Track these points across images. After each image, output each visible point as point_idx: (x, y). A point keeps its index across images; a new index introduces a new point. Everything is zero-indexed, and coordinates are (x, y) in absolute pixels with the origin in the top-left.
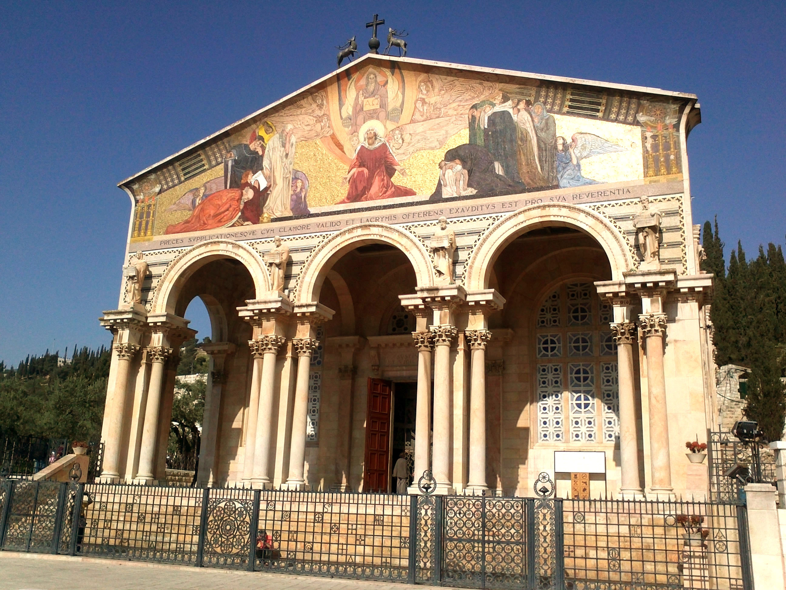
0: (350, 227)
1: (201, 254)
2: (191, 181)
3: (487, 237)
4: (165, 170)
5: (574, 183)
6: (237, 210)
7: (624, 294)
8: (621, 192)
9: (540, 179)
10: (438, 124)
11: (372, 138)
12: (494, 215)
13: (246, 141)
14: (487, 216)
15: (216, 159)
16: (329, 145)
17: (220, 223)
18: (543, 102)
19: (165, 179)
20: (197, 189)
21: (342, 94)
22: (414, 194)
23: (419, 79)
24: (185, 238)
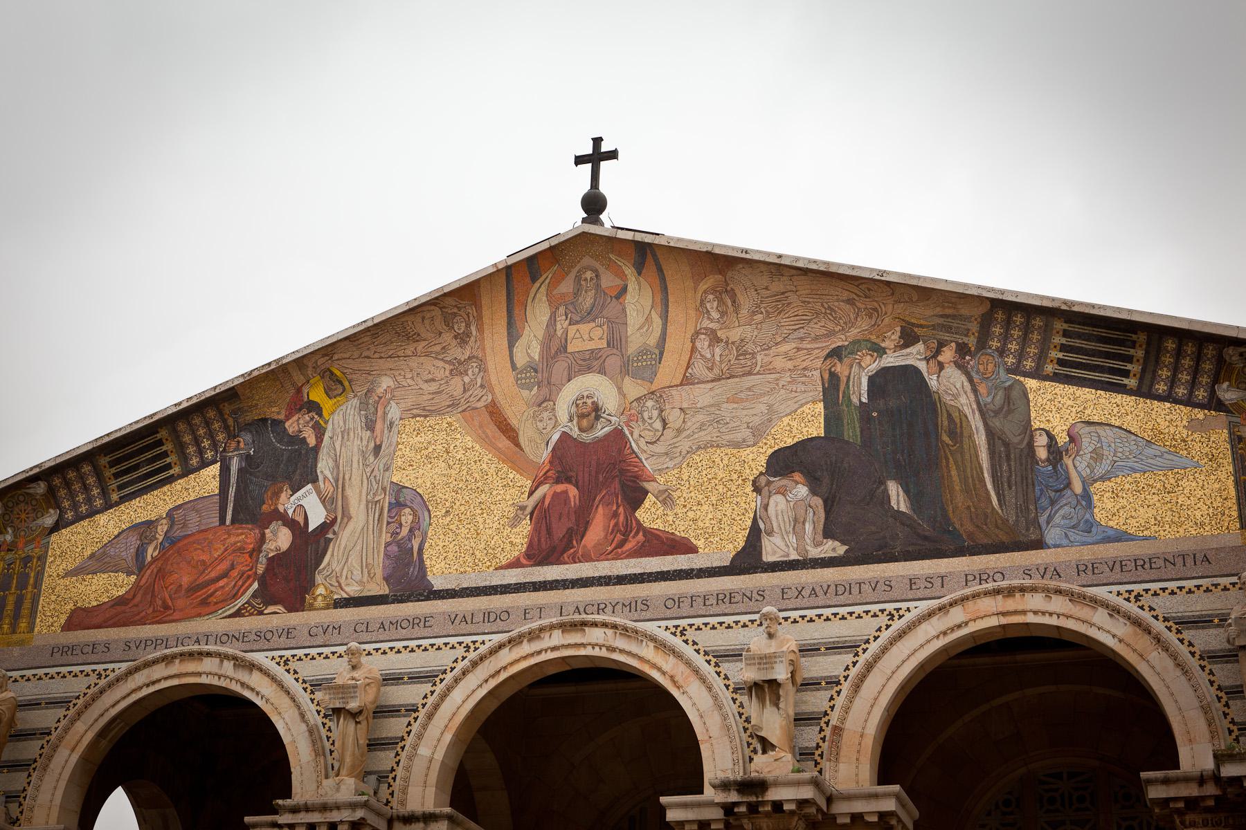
0: (535, 625)
1: (154, 683)
2: (136, 502)
3: (877, 658)
4: (71, 475)
5: (1078, 538)
6: (249, 577)
7: (1211, 803)
8: (1189, 561)
9: (997, 527)
10: (749, 389)
11: (589, 414)
12: (890, 607)
13: (277, 413)
14: (875, 608)
15: (201, 452)
16: (481, 426)
17: (206, 606)
18: (997, 349)
19: (72, 495)
20: (150, 524)
21: (516, 311)
22: (692, 549)
23: (703, 286)
24: (117, 640)
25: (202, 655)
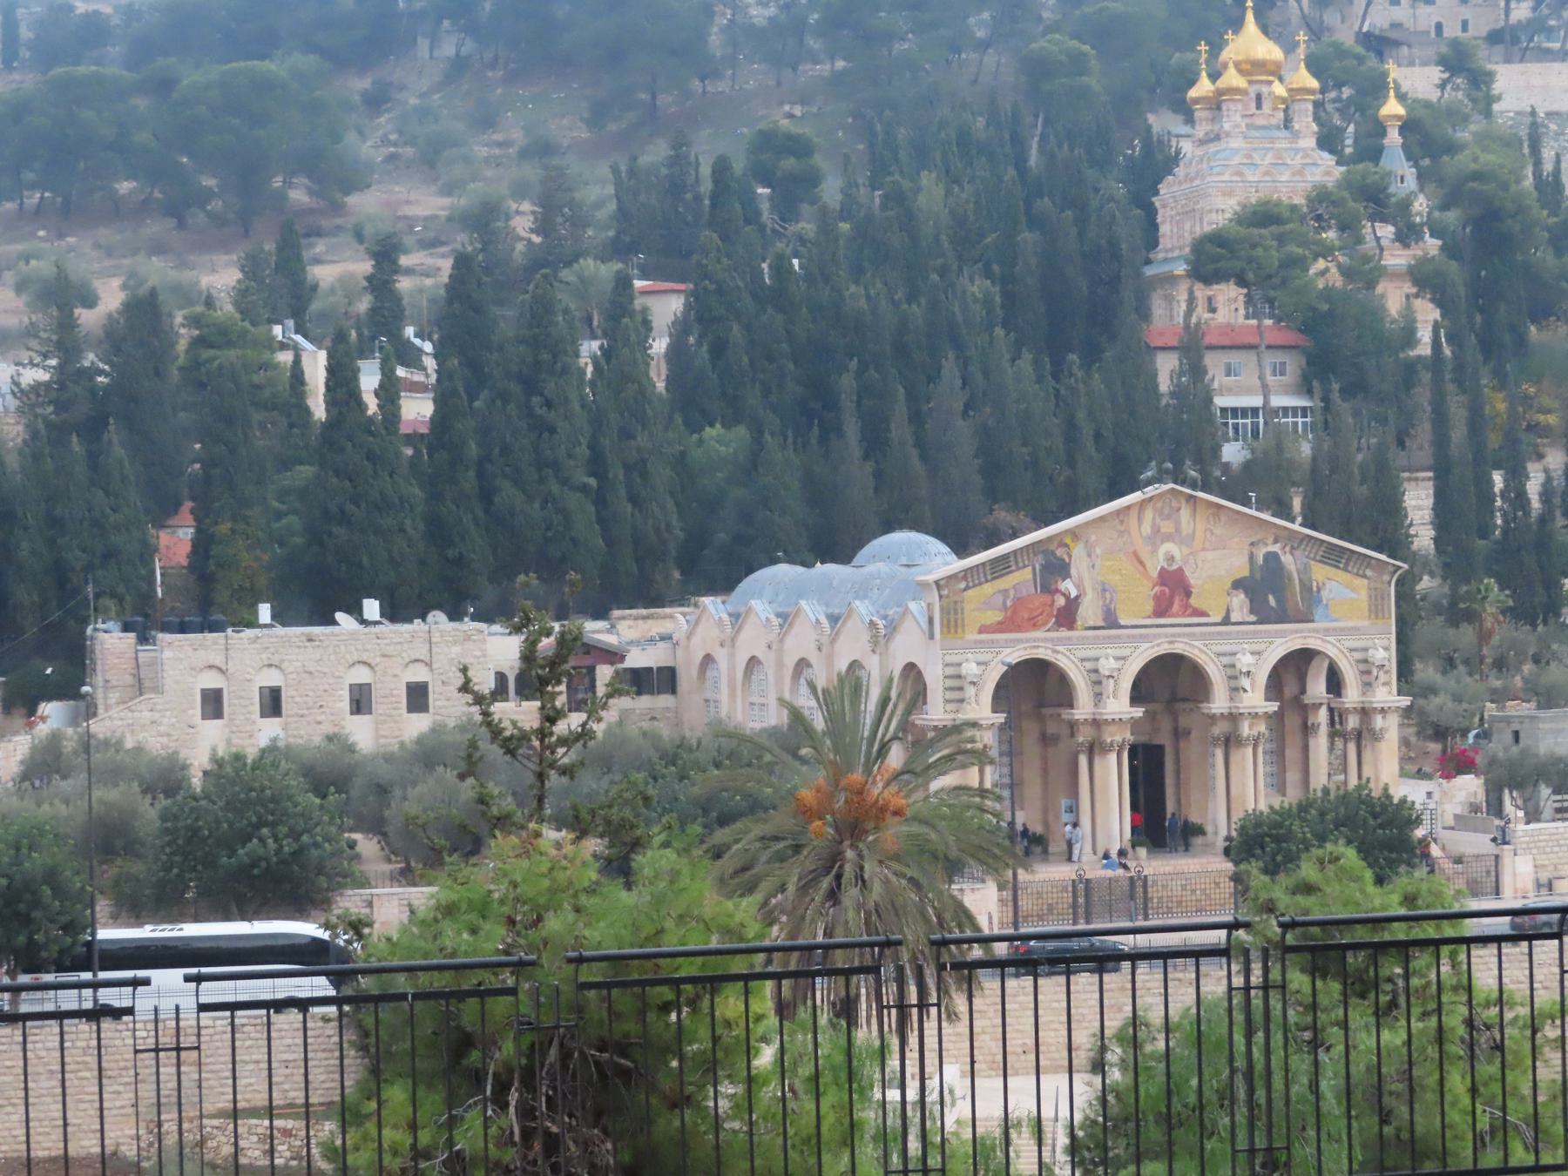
13: (1052, 547)
17: (1035, 626)
25: (1038, 647)
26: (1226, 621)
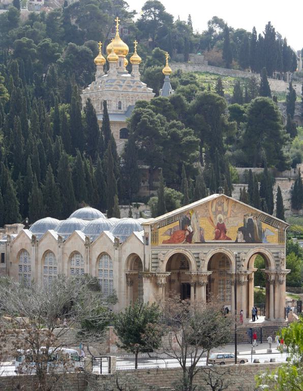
2: (169, 225)
17: (180, 242)
20: (171, 229)
26: (236, 242)
